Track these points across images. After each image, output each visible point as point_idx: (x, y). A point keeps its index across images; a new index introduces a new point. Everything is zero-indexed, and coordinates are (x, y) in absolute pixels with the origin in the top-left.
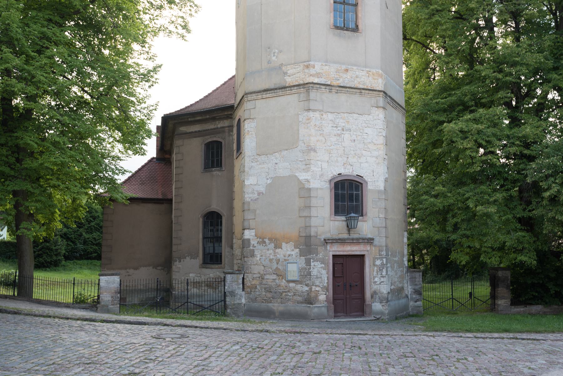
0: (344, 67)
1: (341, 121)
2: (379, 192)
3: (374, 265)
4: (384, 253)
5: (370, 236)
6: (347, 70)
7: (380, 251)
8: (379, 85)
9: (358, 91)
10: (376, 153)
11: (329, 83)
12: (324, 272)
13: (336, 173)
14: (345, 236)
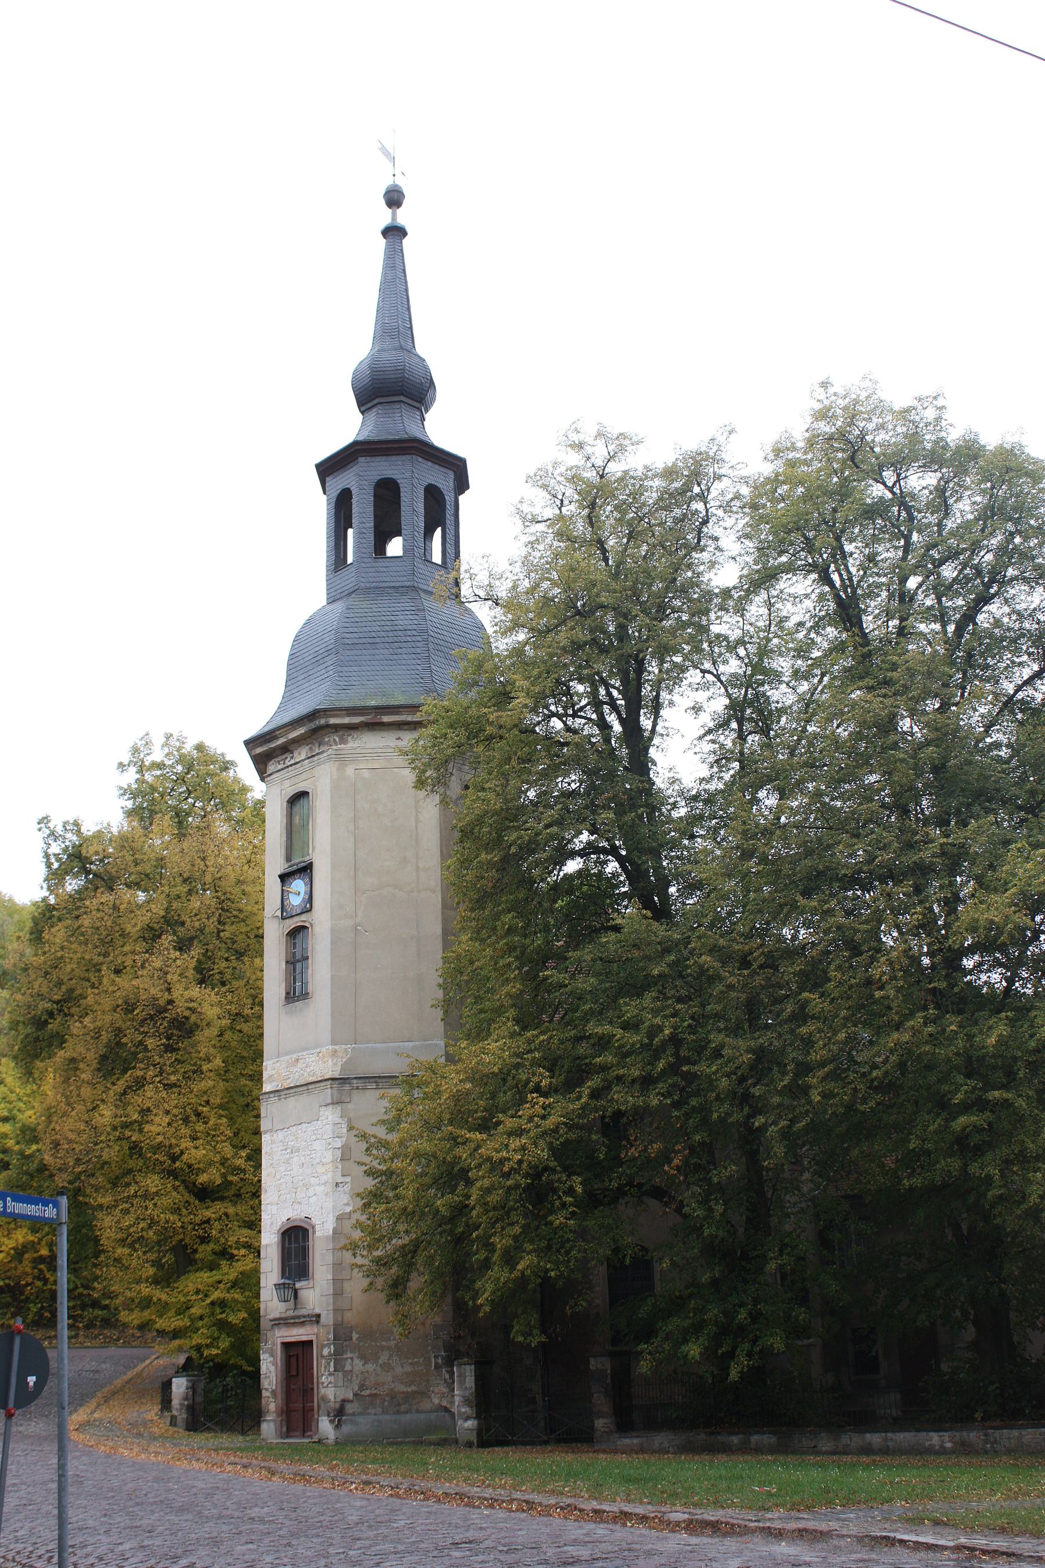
0: (295, 1056)
1: (291, 1138)
2: (327, 1237)
3: (322, 1356)
4: (331, 1336)
5: (317, 1311)
6: (297, 1060)
7: (329, 1333)
8: (330, 1068)
9: (305, 1088)
10: (324, 1178)
11: (279, 1088)
12: (272, 1368)
13: (284, 1219)
14: (291, 1313)
